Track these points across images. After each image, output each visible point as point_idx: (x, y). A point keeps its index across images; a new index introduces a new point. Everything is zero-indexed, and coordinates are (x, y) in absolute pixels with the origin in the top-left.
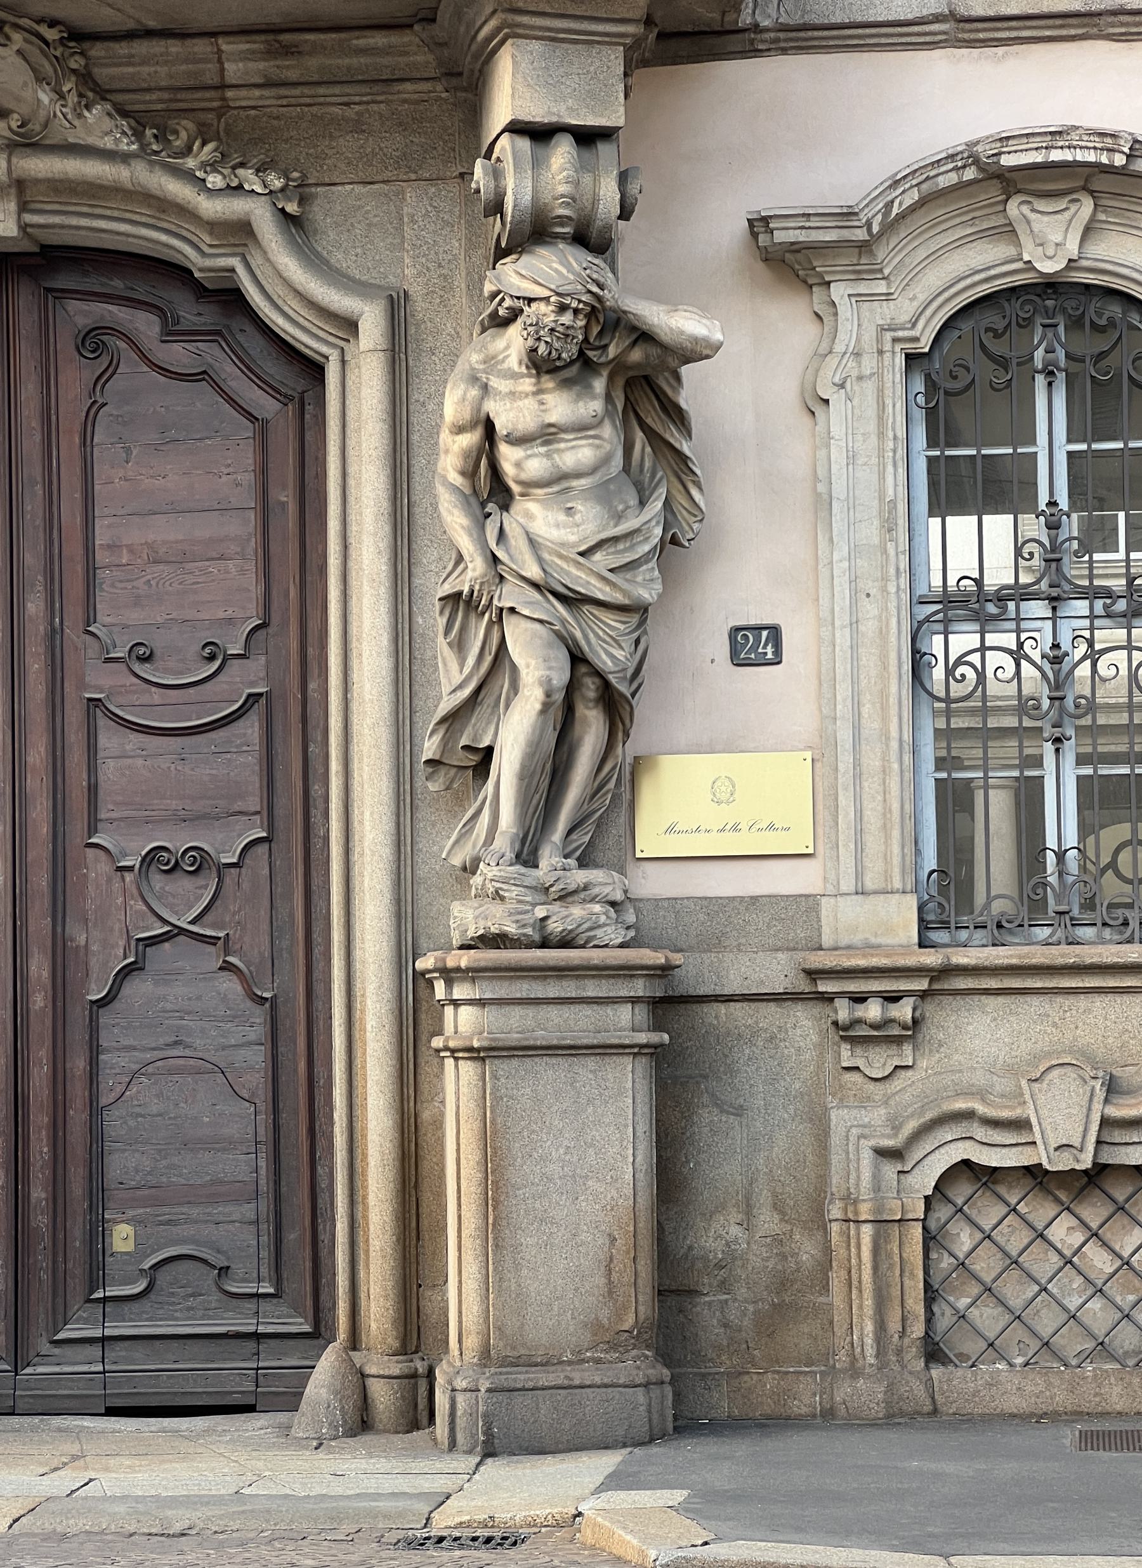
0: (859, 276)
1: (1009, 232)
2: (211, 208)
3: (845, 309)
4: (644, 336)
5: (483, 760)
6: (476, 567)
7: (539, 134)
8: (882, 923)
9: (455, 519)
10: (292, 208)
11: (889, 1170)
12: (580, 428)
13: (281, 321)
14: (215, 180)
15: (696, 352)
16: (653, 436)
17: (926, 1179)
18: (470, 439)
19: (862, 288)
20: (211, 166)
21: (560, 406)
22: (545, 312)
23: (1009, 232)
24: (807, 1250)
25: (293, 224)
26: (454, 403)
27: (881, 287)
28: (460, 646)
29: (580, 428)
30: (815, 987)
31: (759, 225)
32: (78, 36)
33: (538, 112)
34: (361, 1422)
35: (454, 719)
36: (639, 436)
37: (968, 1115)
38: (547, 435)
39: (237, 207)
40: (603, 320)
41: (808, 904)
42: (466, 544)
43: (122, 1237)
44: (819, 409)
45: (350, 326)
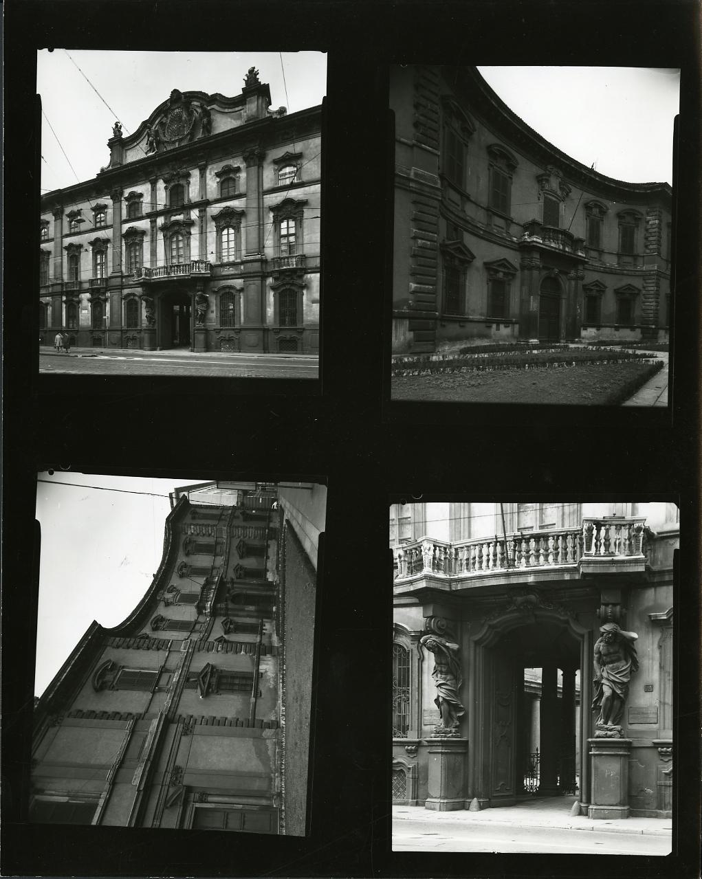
30: (215, 330)
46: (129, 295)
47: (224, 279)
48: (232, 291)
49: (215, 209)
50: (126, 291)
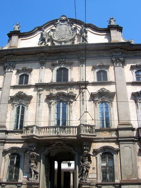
2: (70, 148)
8: (100, 181)
25: (73, 149)
31: (94, 150)
32: (64, 141)
45: (75, 154)
46: (13, 148)
48: (111, 151)
49: (92, 89)
50: (8, 146)
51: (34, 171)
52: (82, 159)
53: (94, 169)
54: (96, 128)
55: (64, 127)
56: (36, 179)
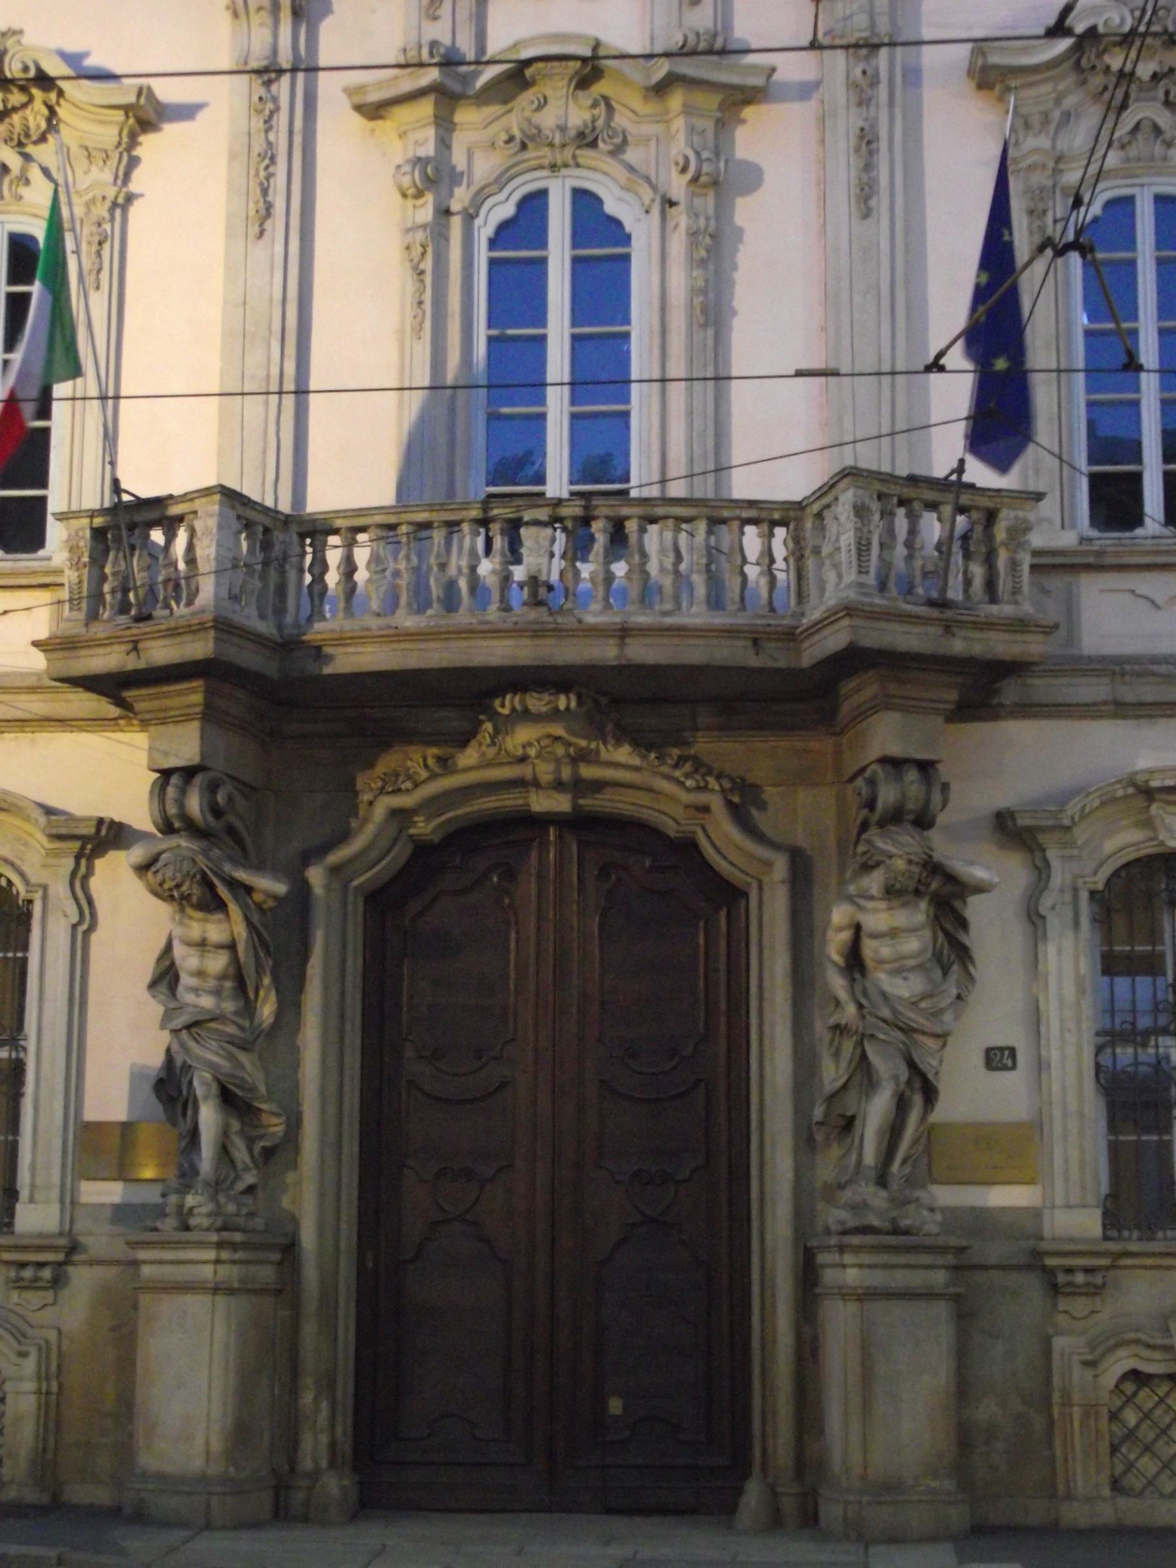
0: (1064, 845)
1: (1148, 823)
3: (1056, 865)
4: (951, 878)
5: (848, 1124)
6: (851, 1009)
7: (894, 764)
9: (838, 984)
10: (736, 799)
11: (1089, 1374)
12: (914, 930)
13: (723, 863)
14: (689, 783)
15: (980, 889)
16: (947, 934)
17: (1109, 1379)
18: (846, 936)
19: (1067, 852)
20: (687, 776)
21: (902, 917)
22: (900, 864)
23: (1148, 823)
24: (1039, 1423)
26: (840, 914)
27: (1076, 852)
28: (837, 1055)
29: (914, 930)
33: (895, 749)
34: (775, 1522)
35: (832, 1098)
36: (941, 935)
37: (1137, 1342)
38: (893, 933)
39: (702, 798)
40: (933, 868)
41: (1036, 1213)
42: (843, 995)
43: (615, 1406)
44: (1039, 923)
47: (1120, 709)
51: (228, 1098)
52: (858, 928)
53: (999, 1059)
54: (1037, 540)
55: (603, 513)
56: (250, 1189)
